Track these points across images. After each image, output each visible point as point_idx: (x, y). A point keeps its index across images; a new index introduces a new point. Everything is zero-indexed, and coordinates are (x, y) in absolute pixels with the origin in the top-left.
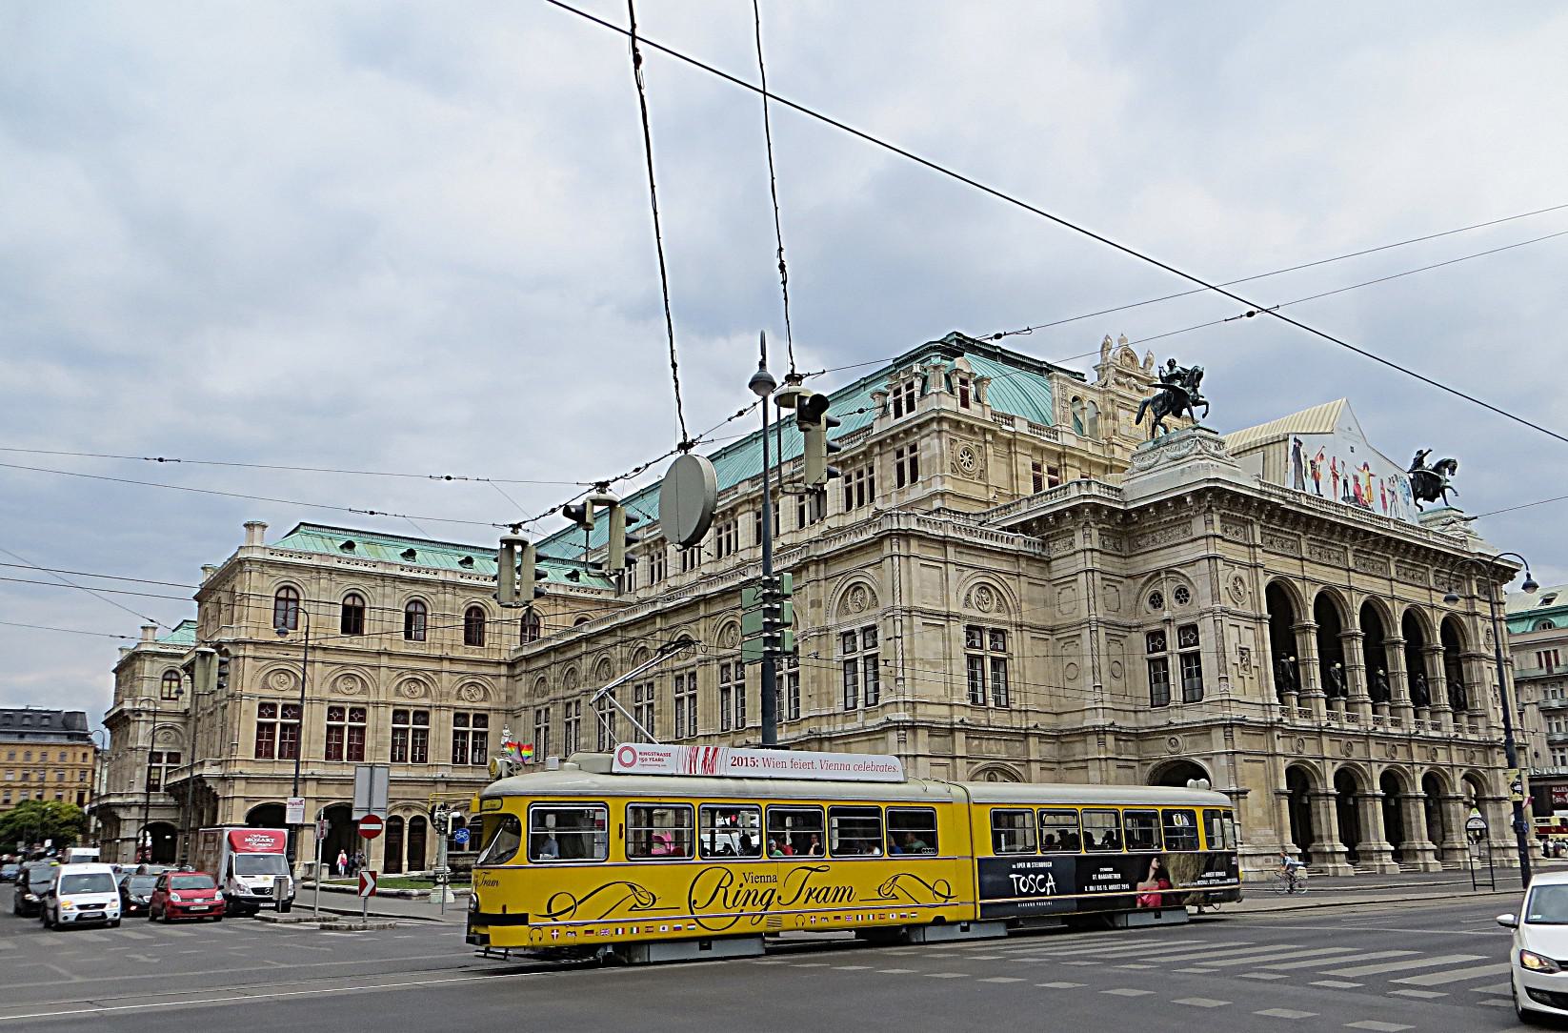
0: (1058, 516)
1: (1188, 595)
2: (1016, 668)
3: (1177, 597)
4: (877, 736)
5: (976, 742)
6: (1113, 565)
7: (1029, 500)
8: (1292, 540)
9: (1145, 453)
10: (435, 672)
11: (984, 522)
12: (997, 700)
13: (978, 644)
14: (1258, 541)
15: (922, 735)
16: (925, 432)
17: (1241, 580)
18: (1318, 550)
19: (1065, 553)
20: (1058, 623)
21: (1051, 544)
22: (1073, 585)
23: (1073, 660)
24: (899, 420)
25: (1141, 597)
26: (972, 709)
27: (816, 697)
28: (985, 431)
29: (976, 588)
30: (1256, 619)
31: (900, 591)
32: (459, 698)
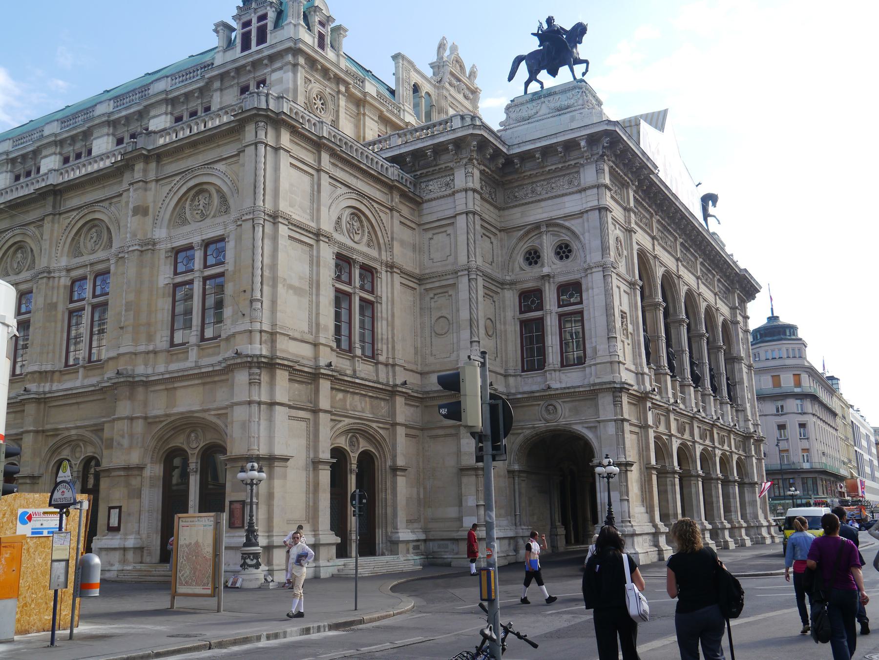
1: (570, 251)
2: (384, 315)
3: (557, 253)
4: (217, 379)
6: (490, 214)
15: (282, 376)
16: (278, 65)
19: (441, 194)
20: (427, 271)
21: (423, 186)
22: (450, 230)
23: (444, 313)
25: (516, 252)
27: (130, 329)
28: (338, 80)
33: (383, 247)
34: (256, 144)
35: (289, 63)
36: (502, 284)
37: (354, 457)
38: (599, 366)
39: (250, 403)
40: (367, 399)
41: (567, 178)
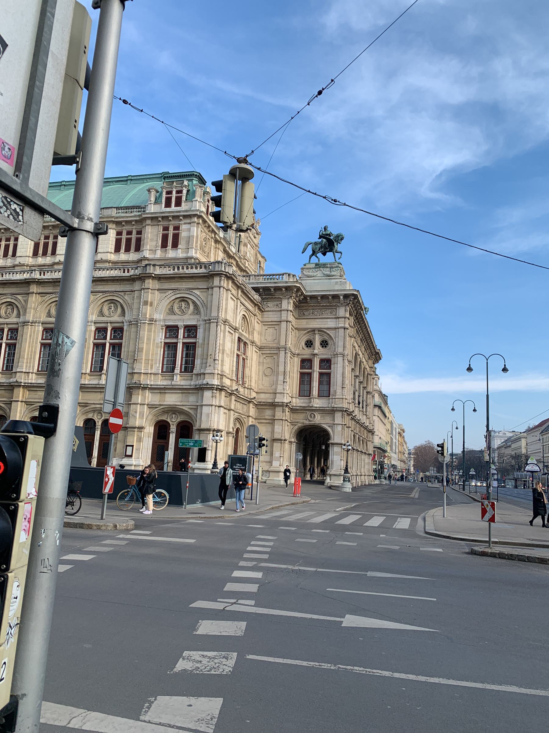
1: (327, 344)
2: (248, 366)
3: (321, 344)
9: (310, 268)
22: (277, 327)
24: (168, 209)
34: (220, 287)
35: (195, 222)
38: (336, 399)
41: (330, 310)
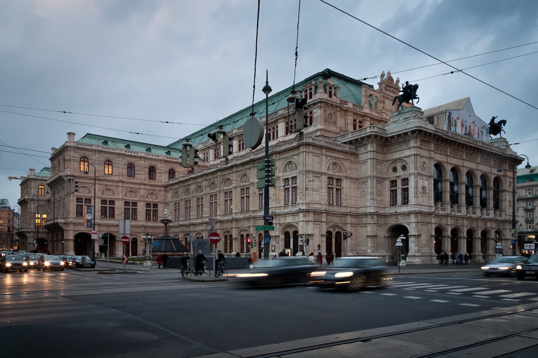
0: (363, 138)
1: (406, 168)
3: (402, 168)
4: (296, 214)
5: (329, 217)
6: (380, 157)
7: (352, 133)
8: (444, 149)
10: (139, 189)
11: (335, 140)
12: (337, 203)
13: (331, 183)
14: (432, 149)
15: (311, 215)
17: (425, 163)
18: (453, 152)
21: (359, 149)
22: (366, 164)
23: (364, 190)
26: (329, 206)
28: (337, 106)
29: (332, 164)
30: (429, 176)
31: (306, 164)
32: (147, 198)
33: (344, 172)
34: (303, 152)
36: (384, 179)
37: (334, 234)
39: (303, 221)
40: (338, 217)
